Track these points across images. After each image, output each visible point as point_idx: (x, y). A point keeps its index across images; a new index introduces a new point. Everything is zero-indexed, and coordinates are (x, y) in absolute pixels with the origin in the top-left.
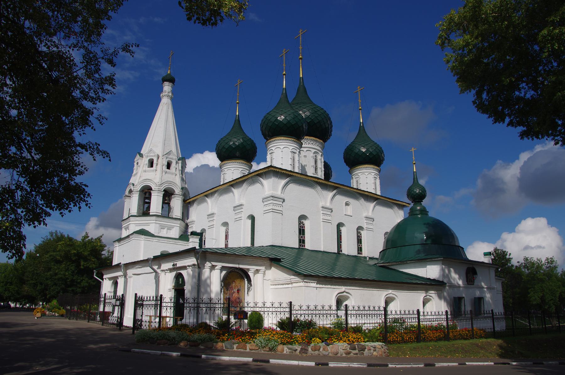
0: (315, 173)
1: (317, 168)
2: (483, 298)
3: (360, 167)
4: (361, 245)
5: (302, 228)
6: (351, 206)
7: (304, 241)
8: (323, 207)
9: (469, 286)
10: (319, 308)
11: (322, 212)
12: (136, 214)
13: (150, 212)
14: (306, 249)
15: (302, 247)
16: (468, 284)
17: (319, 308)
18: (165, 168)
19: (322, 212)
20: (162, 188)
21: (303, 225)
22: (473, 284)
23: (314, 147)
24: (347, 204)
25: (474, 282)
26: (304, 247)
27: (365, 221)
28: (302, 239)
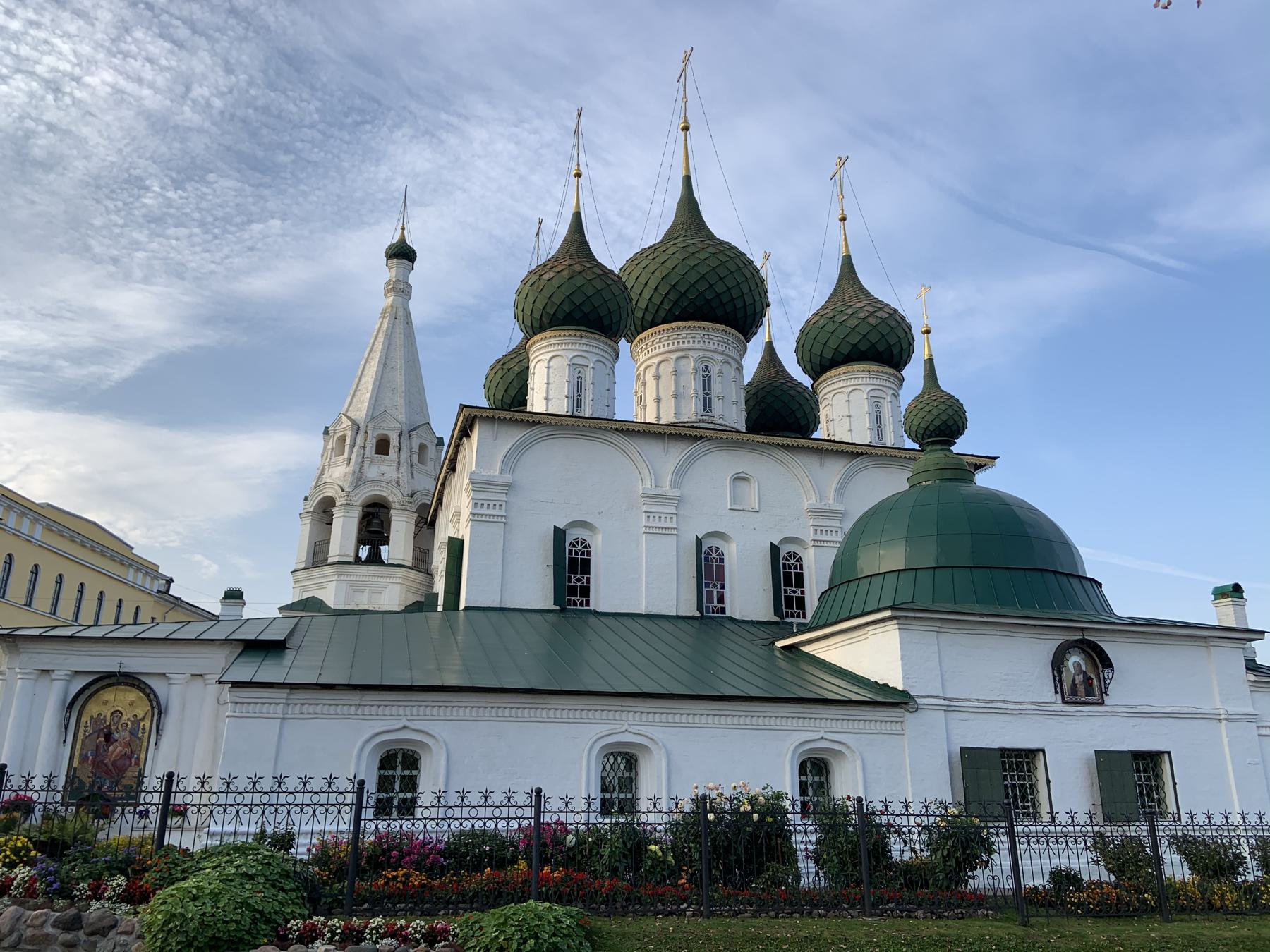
0: (702, 412)
1: (710, 399)
2: (1169, 753)
3: (828, 374)
4: (803, 592)
5: (583, 554)
6: (754, 485)
7: (586, 592)
8: (645, 495)
9: (1067, 708)
10: (242, 784)
11: (645, 508)
12: (303, 566)
13: (330, 554)
14: (595, 613)
15: (579, 607)
16: (1064, 702)
17: (242, 784)
18: (370, 450)
19: (645, 508)
20: (356, 499)
21: (585, 547)
22: (1102, 703)
23: (697, 345)
24: (739, 478)
25: (1104, 693)
26: (588, 604)
27: (811, 522)
28: (579, 584)
